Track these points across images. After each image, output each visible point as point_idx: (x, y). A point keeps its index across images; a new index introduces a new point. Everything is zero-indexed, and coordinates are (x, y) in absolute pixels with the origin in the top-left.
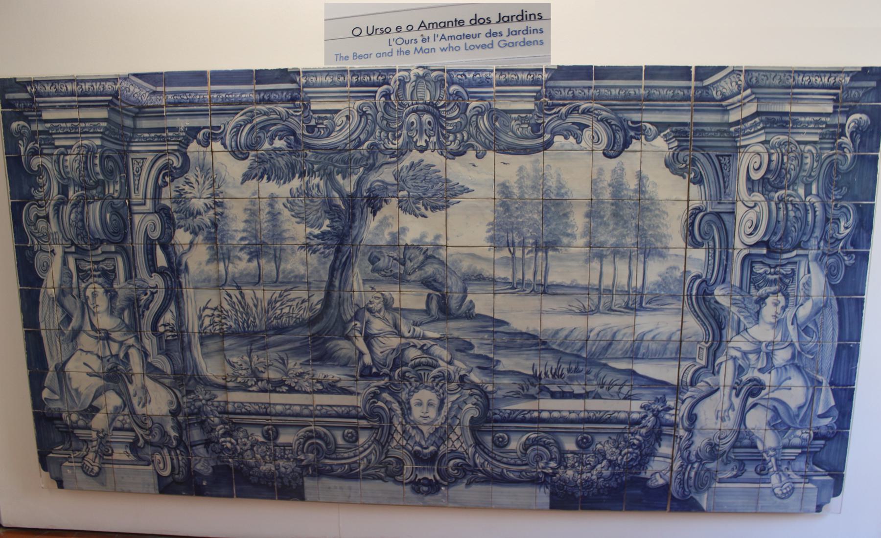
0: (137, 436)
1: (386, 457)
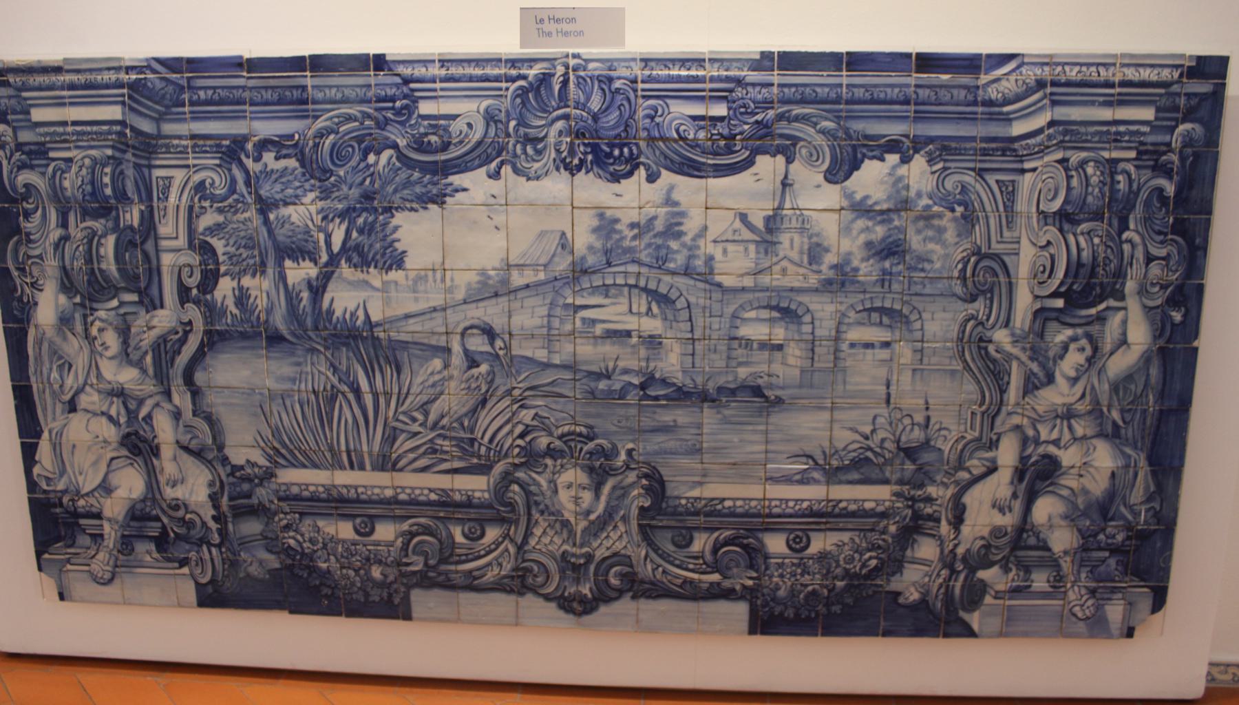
1: (524, 561)
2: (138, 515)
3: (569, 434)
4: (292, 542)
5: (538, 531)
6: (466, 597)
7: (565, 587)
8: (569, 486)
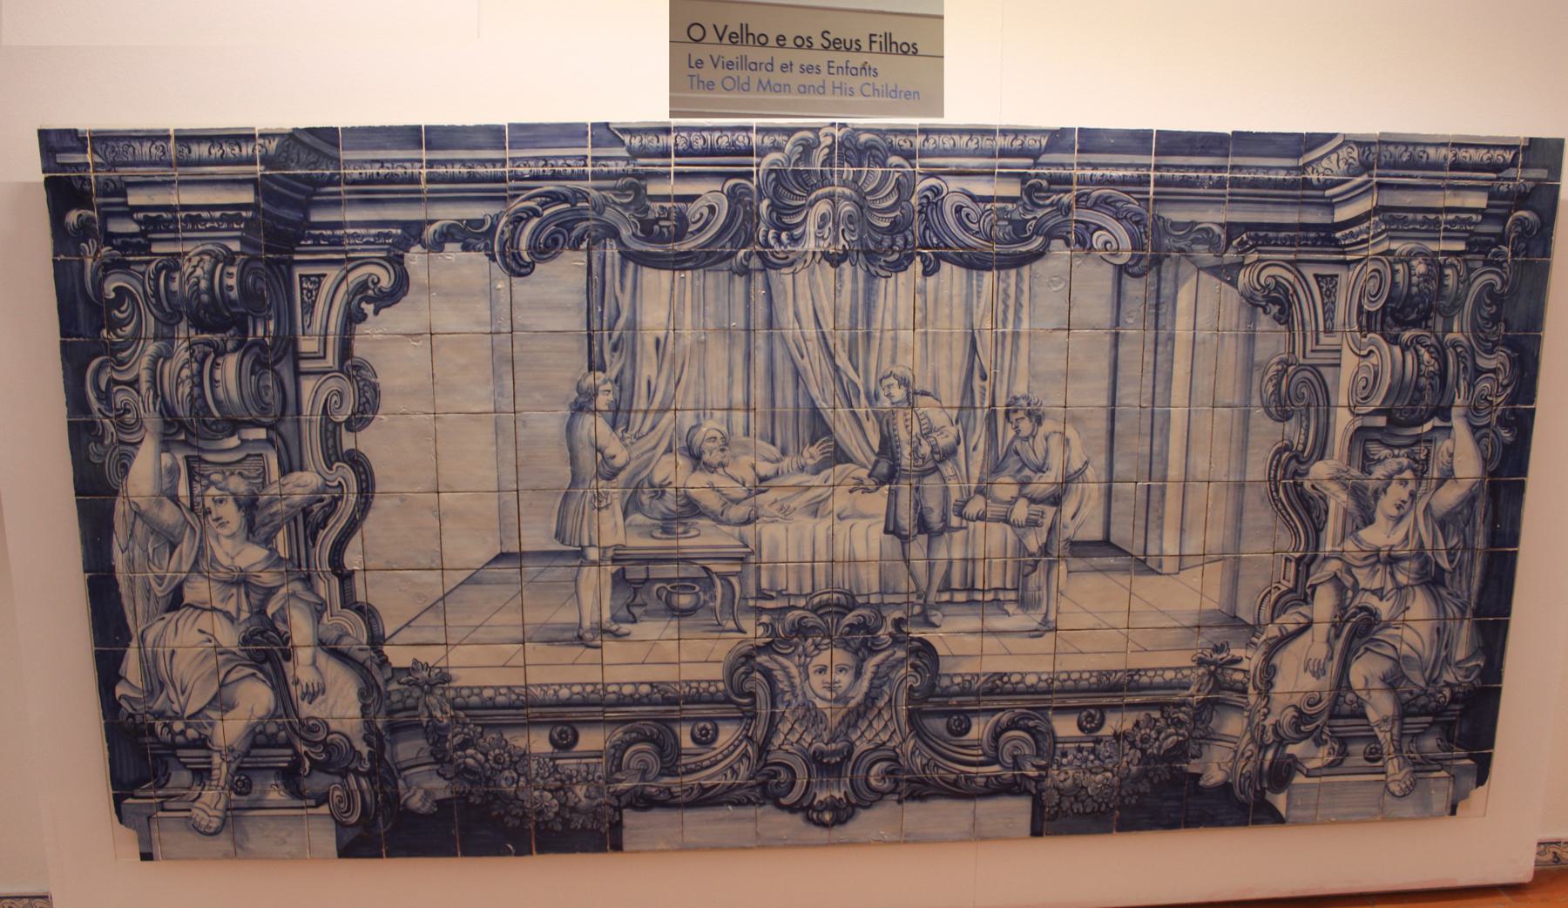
0: (296, 753)
1: (765, 765)
2: (258, 739)
3: (827, 604)
4: (470, 761)
5: (784, 727)
6: (689, 815)
7: (815, 795)
8: (822, 670)
